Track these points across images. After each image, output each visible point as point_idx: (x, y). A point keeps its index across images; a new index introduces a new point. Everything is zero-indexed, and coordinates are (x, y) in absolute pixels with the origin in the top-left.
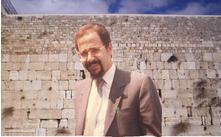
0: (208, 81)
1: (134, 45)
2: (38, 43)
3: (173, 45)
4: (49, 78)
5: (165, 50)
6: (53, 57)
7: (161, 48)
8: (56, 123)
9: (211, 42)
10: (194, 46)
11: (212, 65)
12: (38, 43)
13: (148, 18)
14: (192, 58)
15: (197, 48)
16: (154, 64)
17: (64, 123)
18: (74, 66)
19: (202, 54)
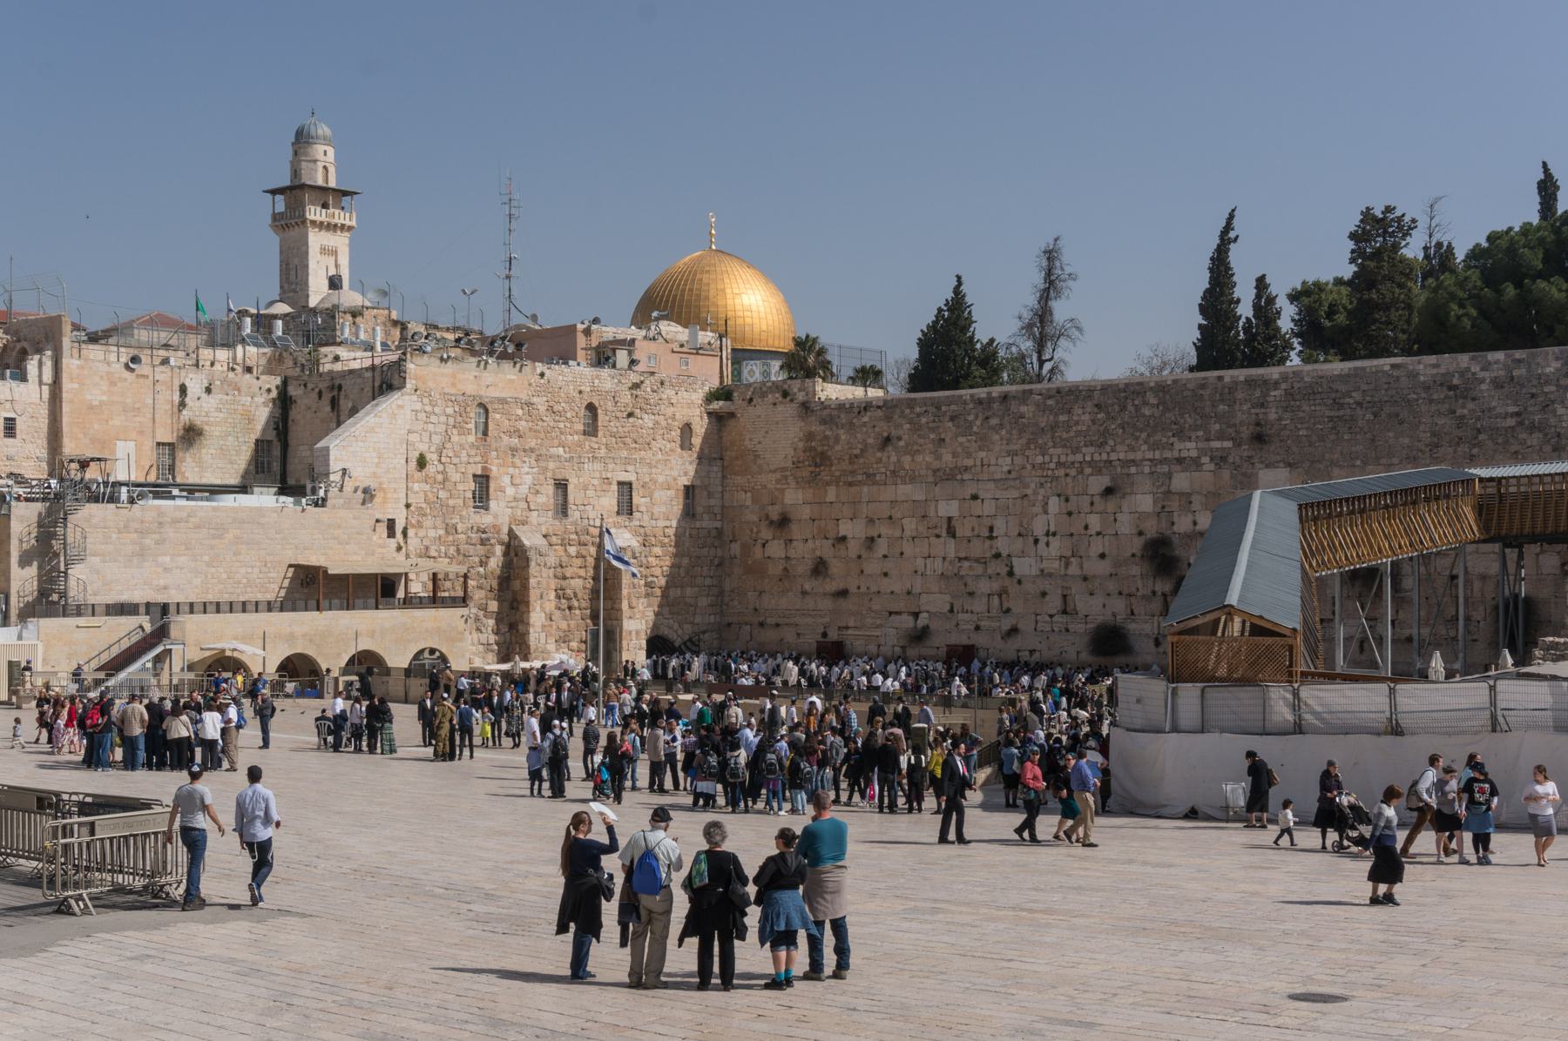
0: (1176, 540)
1: (1039, 459)
2: (881, 459)
3: (1113, 456)
4: (898, 533)
5: (1098, 471)
6: (905, 491)
8: (911, 619)
9: (1192, 445)
11: (1186, 498)
12: (880, 461)
15: (1164, 461)
16: (1073, 499)
17: (923, 620)
18: (936, 506)
19: (1169, 476)
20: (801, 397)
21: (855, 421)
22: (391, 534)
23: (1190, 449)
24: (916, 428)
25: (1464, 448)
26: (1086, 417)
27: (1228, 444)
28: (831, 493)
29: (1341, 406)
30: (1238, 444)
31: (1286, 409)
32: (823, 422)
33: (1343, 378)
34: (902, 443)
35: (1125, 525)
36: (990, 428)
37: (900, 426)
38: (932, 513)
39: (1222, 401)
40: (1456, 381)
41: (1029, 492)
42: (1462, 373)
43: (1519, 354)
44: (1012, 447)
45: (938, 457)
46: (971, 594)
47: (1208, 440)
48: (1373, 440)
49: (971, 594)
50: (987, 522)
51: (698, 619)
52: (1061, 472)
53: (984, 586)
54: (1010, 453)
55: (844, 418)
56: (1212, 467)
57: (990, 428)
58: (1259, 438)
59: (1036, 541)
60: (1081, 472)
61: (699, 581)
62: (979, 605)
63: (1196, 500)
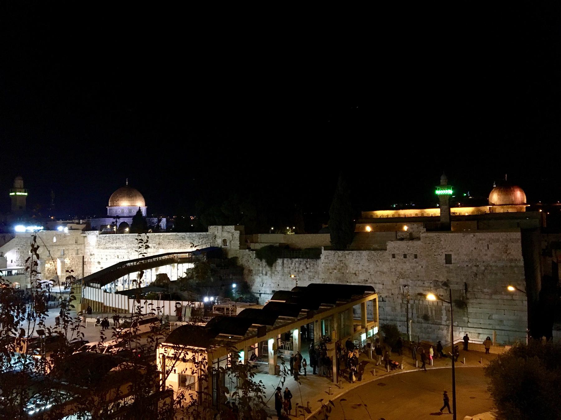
20: (96, 234)
22: (12, 262)
24: (113, 240)
25: (184, 247)
29: (169, 240)
31: (163, 240)
32: (100, 238)
37: (111, 240)
43: (191, 233)
50: (123, 256)
51: (79, 272)
52: (133, 248)
54: (127, 245)
55: (103, 238)
56: (153, 248)
58: (159, 244)
61: (79, 265)
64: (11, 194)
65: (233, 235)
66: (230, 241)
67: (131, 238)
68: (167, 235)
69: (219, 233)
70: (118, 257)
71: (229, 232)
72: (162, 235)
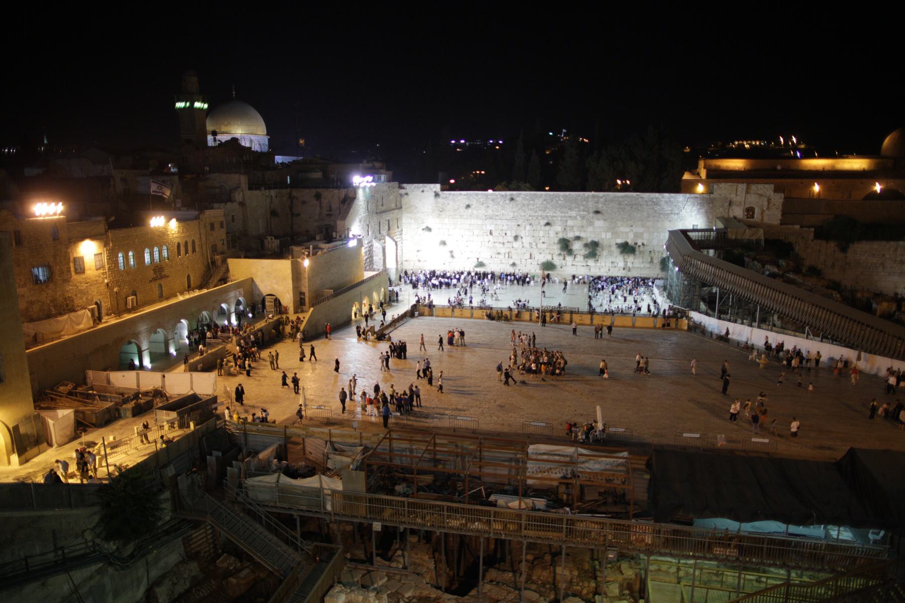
1: (523, 214)
3: (548, 215)
7: (540, 216)
10: (563, 215)
11: (572, 227)
13: (534, 195)
14: (560, 223)
15: (565, 217)
19: (567, 221)
20: (434, 190)
21: (456, 199)
23: (573, 213)
26: (540, 202)
27: (586, 213)
28: (446, 221)
29: (621, 205)
30: (588, 213)
31: (604, 204)
32: (443, 198)
33: (622, 197)
34: (473, 207)
35: (552, 234)
36: (506, 204)
38: (485, 228)
39: (584, 200)
40: (655, 200)
41: (519, 223)
42: (656, 198)
43: (673, 195)
44: (513, 210)
45: (487, 212)
46: (499, 253)
47: (579, 211)
48: (630, 215)
49: (499, 253)
52: (531, 218)
53: (503, 251)
55: (451, 197)
57: (506, 204)
59: (522, 238)
60: (537, 218)
62: (501, 257)
63: (575, 229)
64: (180, 105)
65: (769, 200)
66: (763, 212)
67: (528, 200)
68: (615, 197)
69: (739, 197)
70: (491, 233)
71: (761, 195)
72: (604, 196)
